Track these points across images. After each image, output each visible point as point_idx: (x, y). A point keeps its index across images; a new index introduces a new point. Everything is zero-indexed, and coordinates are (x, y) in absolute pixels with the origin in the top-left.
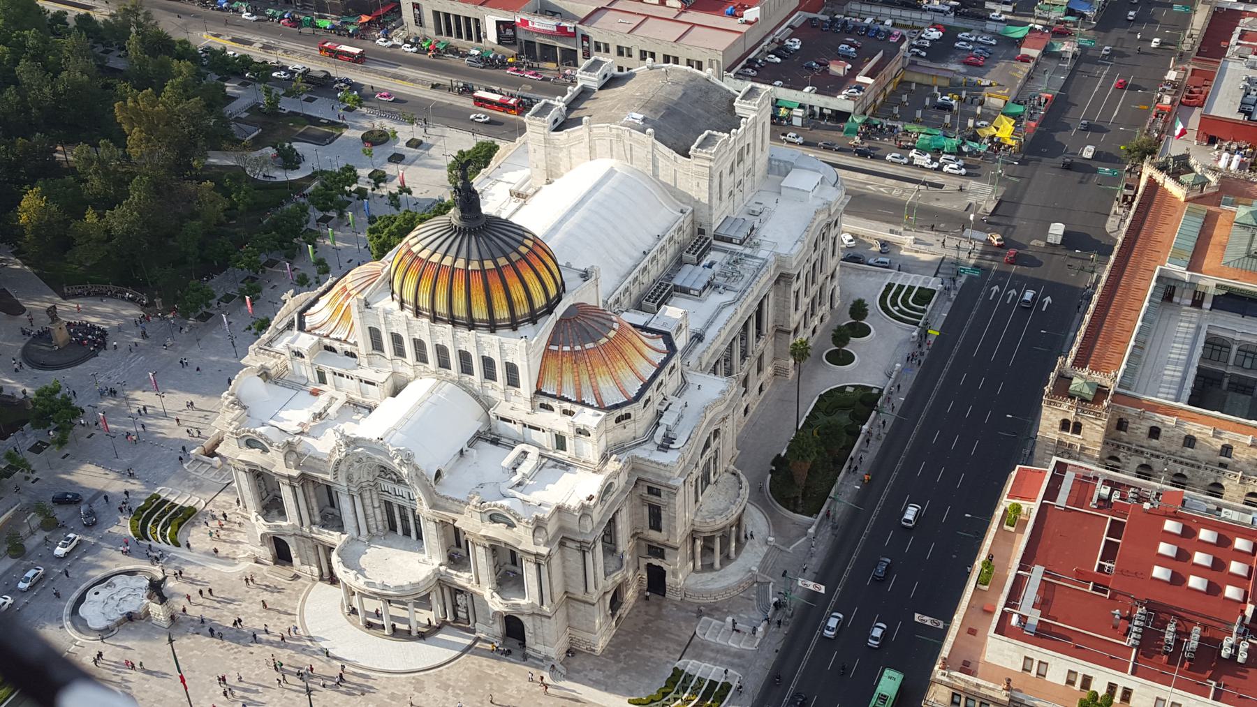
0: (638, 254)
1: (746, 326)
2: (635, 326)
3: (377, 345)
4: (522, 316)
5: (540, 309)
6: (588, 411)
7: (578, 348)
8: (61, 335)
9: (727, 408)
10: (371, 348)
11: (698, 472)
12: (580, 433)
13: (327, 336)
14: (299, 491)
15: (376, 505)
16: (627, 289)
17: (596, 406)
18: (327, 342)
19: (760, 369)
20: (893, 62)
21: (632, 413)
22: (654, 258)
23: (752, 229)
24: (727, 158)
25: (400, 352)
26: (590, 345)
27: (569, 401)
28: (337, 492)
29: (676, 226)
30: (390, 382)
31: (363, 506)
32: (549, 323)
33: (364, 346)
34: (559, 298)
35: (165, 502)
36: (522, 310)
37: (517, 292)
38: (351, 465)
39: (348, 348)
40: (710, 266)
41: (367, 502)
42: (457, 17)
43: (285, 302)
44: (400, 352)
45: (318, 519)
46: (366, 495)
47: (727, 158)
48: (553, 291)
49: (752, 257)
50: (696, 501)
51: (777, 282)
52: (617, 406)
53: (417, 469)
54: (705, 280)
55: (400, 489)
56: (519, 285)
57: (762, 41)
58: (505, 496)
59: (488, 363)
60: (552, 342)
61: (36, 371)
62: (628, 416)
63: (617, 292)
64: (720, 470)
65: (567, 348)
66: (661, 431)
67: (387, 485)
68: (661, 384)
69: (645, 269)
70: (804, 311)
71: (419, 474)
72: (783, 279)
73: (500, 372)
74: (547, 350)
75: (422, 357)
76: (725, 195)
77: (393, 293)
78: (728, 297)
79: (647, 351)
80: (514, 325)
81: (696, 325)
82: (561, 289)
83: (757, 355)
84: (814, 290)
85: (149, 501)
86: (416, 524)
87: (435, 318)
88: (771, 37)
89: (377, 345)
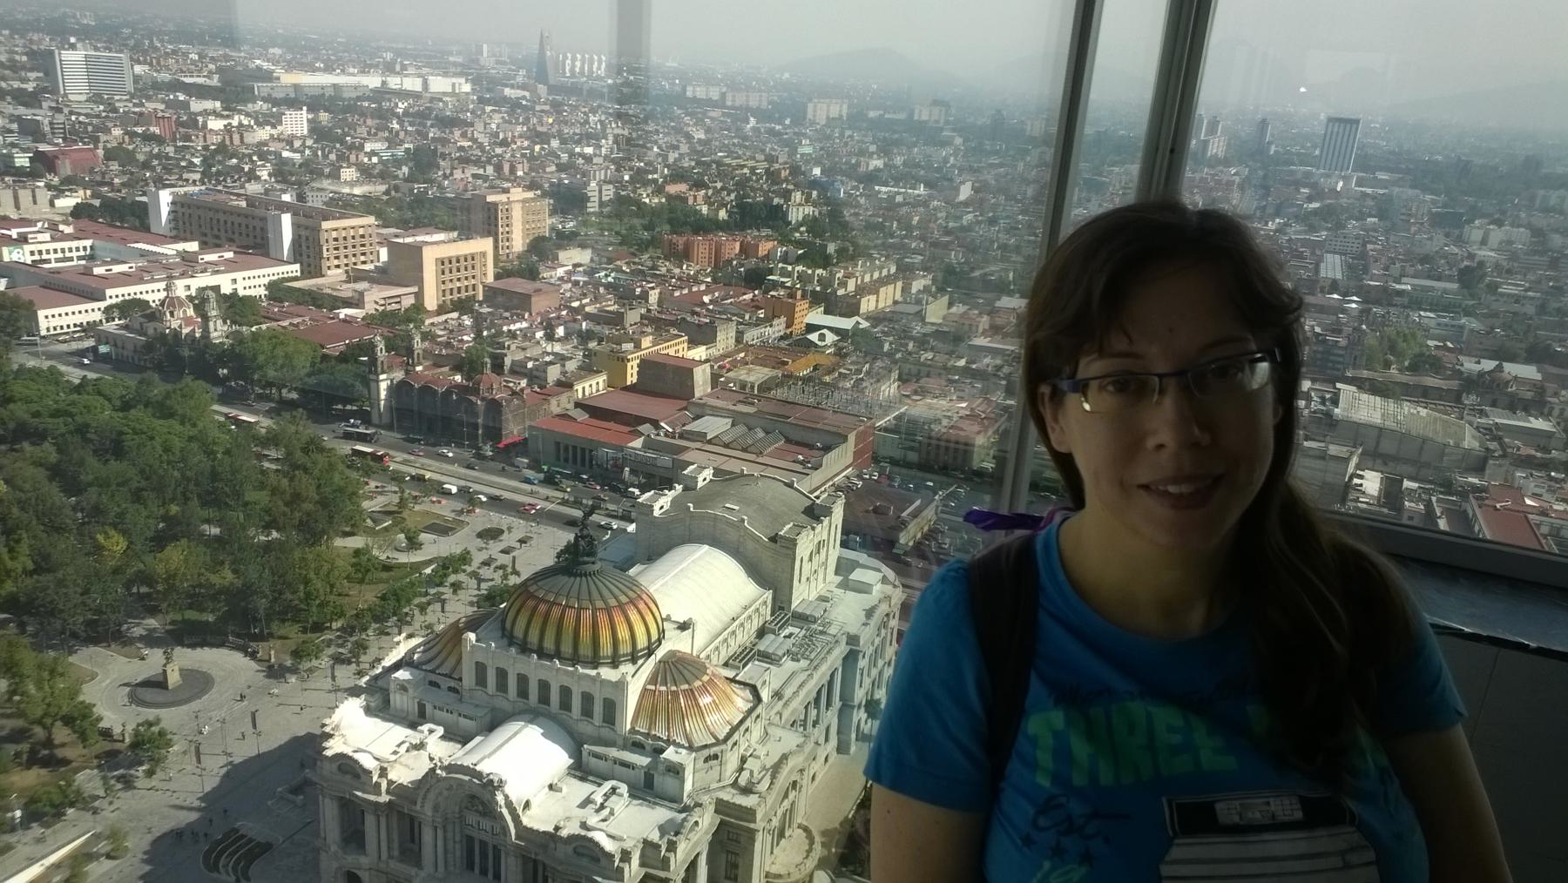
0: (727, 619)
1: (819, 692)
2: (727, 678)
3: (481, 680)
4: (624, 656)
5: (642, 650)
6: (680, 750)
7: (674, 688)
8: (174, 678)
9: (806, 759)
10: (474, 683)
11: (775, 822)
12: (669, 771)
13: (433, 671)
14: (383, 820)
15: (457, 839)
16: (717, 648)
17: (687, 745)
18: (433, 677)
19: (827, 740)
20: (929, 508)
21: (720, 754)
22: (742, 625)
23: (825, 611)
24: (807, 547)
25: (502, 686)
26: (686, 687)
27: (660, 739)
28: (420, 823)
29: (761, 599)
30: (489, 716)
31: (445, 839)
32: (649, 666)
33: (468, 679)
34: (659, 641)
35: (243, 836)
36: (625, 648)
37: (623, 633)
38: (440, 794)
39: (453, 684)
40: (789, 636)
41: (450, 835)
42: (575, 448)
43: (398, 643)
44: (502, 686)
45: (396, 853)
46: (450, 827)
47: (807, 547)
48: (655, 637)
49: (822, 633)
50: (772, 853)
51: (845, 659)
52: (706, 746)
53: (506, 797)
54: (785, 648)
55: (486, 824)
56: (625, 626)
57: (824, 484)
58: (588, 829)
59: (587, 699)
60: (653, 679)
61: (139, 709)
62: (716, 757)
63: (708, 649)
64: (795, 825)
65: (663, 688)
66: (745, 775)
67: (472, 818)
68: (747, 730)
69: (734, 632)
70: (867, 686)
71: (509, 804)
72: (851, 658)
73: (598, 709)
74: (645, 690)
75: (523, 693)
76: (804, 579)
77: (503, 629)
78: (804, 663)
79: (734, 696)
80: (615, 664)
81: (776, 685)
82: (662, 633)
83: (826, 726)
84: (874, 672)
85: (226, 836)
86: (494, 858)
87: (542, 654)
88: (831, 483)
89: (481, 680)
